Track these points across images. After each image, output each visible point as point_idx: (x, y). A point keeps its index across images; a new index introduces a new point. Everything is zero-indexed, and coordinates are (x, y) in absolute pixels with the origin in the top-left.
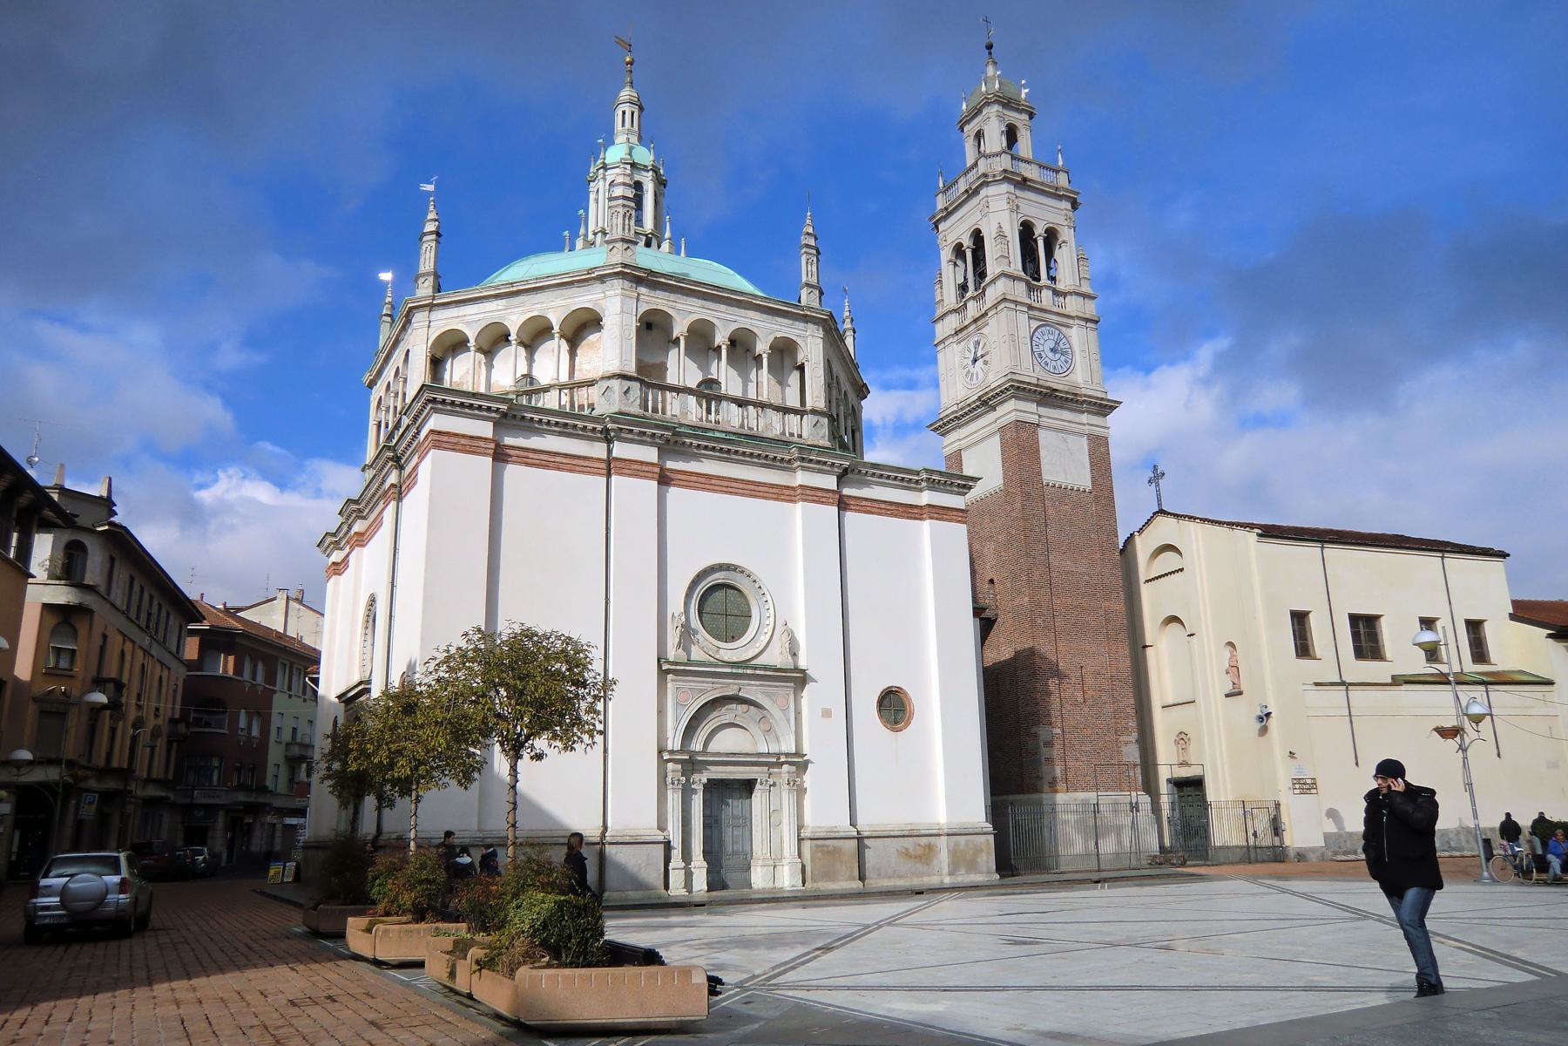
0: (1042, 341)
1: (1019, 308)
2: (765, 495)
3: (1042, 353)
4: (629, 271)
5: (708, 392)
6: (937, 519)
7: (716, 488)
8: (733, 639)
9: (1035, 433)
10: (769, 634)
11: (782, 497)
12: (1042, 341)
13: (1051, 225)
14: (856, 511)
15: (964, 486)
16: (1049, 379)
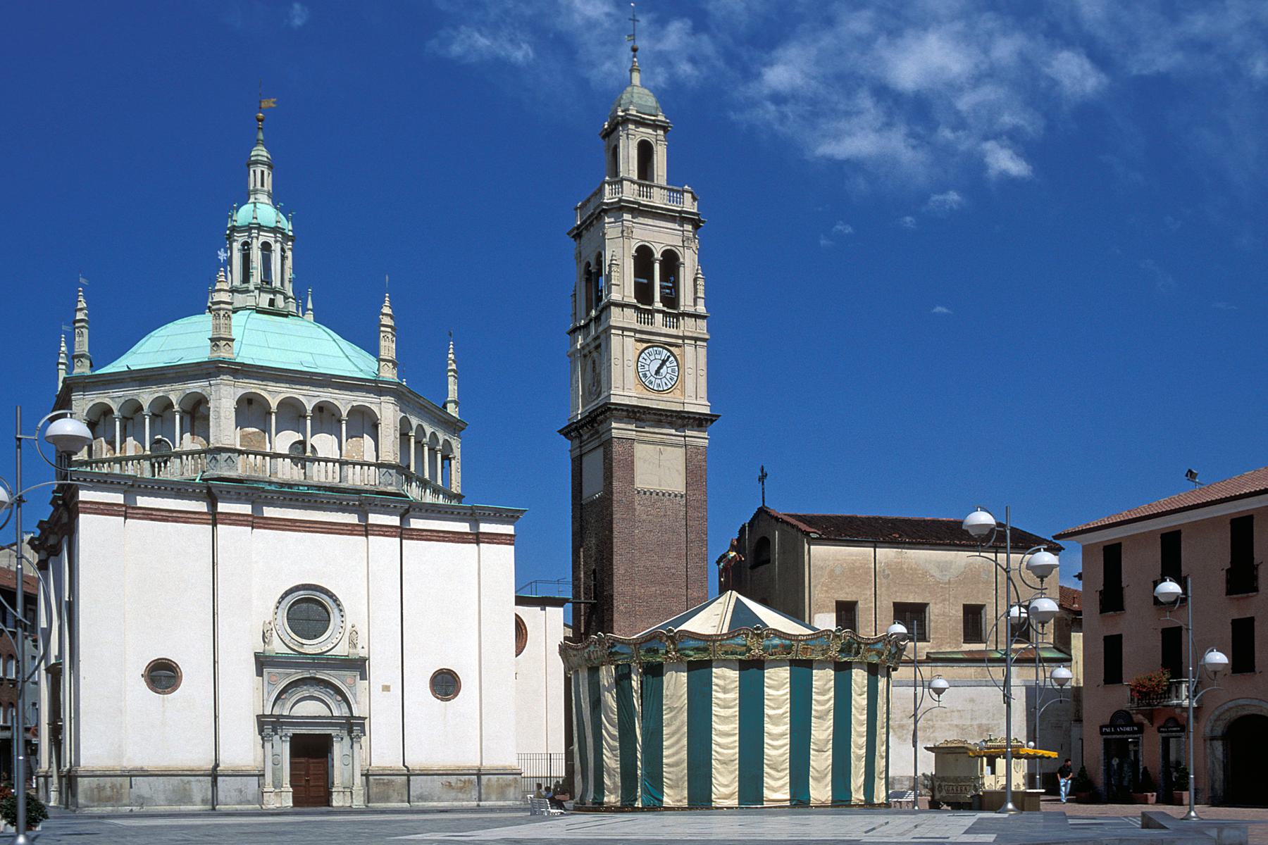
0: (648, 362)
1: (625, 333)
2: (341, 532)
3: (647, 373)
4: (240, 368)
5: (300, 455)
6: (488, 543)
7: (301, 529)
8: (316, 637)
9: (632, 447)
10: (342, 634)
11: (355, 532)
12: (648, 362)
13: (669, 248)
14: (418, 539)
15: (512, 516)
16: (650, 397)
